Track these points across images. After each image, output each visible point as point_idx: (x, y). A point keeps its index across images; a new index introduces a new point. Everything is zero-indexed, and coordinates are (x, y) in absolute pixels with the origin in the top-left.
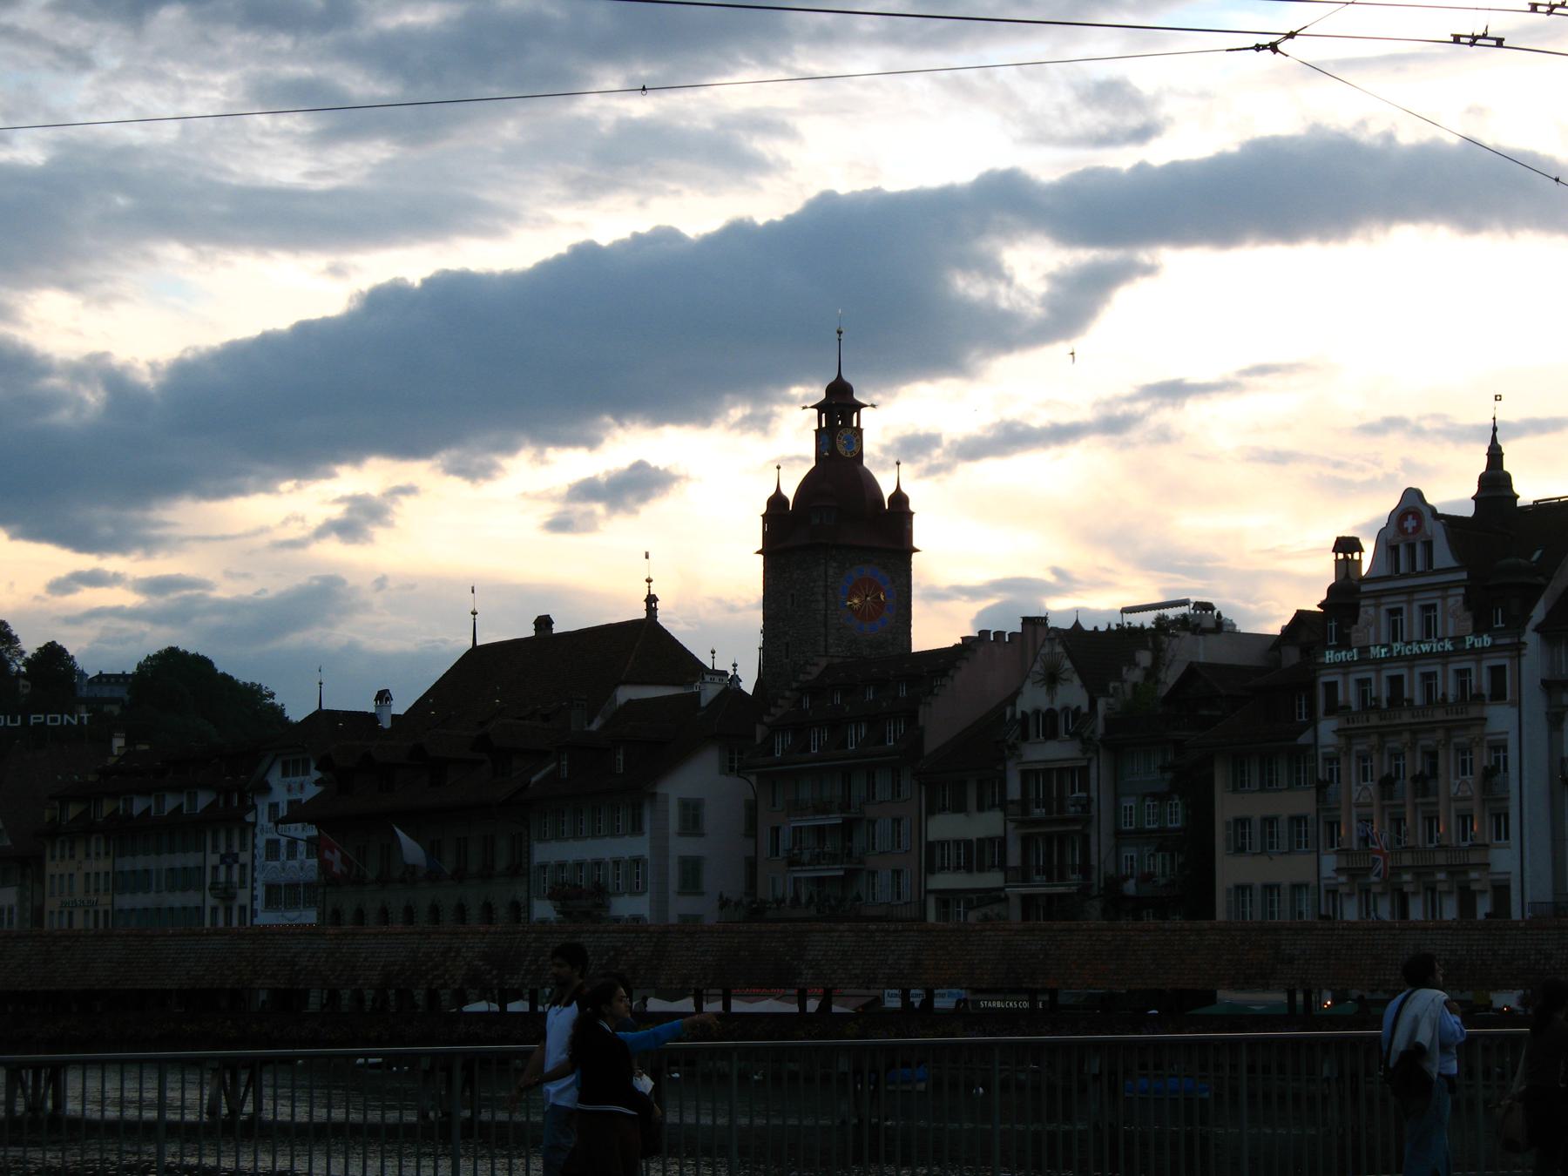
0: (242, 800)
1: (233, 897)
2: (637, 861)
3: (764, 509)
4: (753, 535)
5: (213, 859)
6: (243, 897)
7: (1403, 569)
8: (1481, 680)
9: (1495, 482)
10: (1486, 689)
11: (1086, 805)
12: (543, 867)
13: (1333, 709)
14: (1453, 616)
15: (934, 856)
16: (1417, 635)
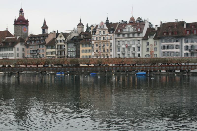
2: (12, 54)
4: (13, 23)
7: (101, 28)
8: (109, 38)
9: (107, 21)
10: (110, 39)
11: (65, 49)
13: (93, 40)
14: (107, 32)
15: (47, 53)
16: (103, 34)
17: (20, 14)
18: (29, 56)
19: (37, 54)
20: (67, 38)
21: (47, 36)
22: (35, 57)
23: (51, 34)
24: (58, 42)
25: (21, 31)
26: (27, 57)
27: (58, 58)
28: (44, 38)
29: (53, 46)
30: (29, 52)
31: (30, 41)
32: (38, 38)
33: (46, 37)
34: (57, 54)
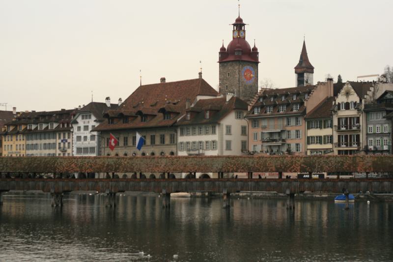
0: (68, 125)
1: (66, 151)
2: (214, 142)
3: (219, 51)
4: (217, 57)
5: (60, 141)
6: (69, 151)
11: (359, 127)
12: (181, 143)
15: (310, 140)
17: (236, 33)
18: (259, 149)
19: (280, 143)
20: (365, 96)
21: (309, 93)
22: (275, 150)
23: (319, 87)
24: (339, 109)
25: (239, 81)
26: (254, 152)
27: (339, 153)
28: (301, 100)
29: (324, 121)
30: (259, 137)
31: (262, 107)
32: (283, 99)
33: (306, 96)
34: (336, 144)
